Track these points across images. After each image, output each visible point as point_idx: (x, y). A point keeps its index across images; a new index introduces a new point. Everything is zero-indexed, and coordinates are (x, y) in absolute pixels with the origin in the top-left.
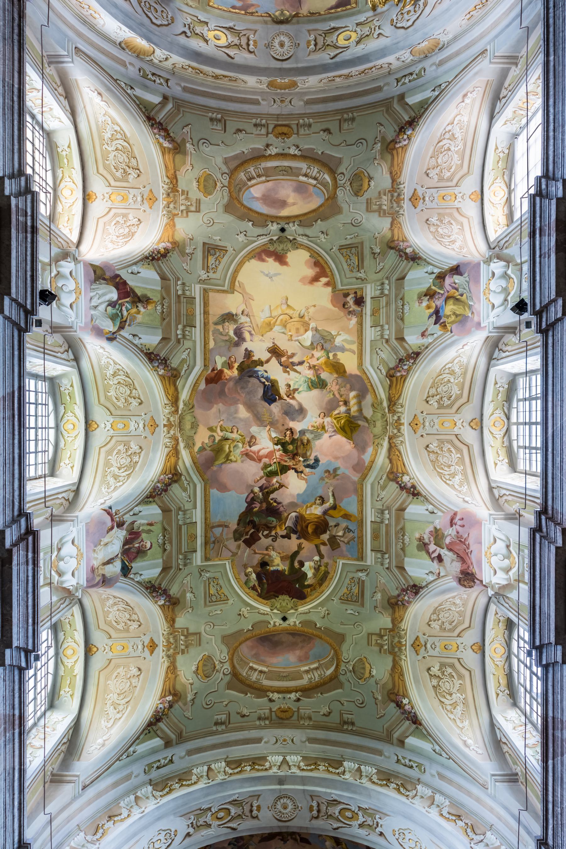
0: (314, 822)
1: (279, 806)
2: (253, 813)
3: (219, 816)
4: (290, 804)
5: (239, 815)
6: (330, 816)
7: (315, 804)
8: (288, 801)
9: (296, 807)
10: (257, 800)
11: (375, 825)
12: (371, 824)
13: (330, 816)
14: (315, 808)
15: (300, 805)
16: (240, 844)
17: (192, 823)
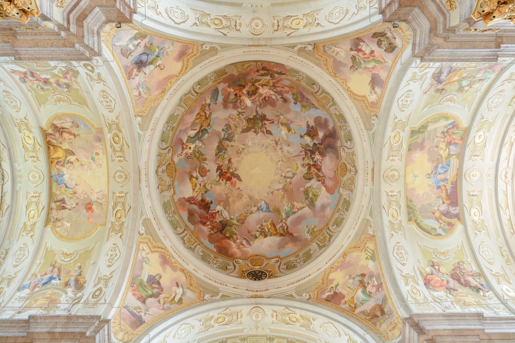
0: (275, 33)
1: (253, 25)
2: (237, 27)
3: (215, 23)
4: (260, 23)
5: (228, 26)
6: (285, 27)
7: (276, 22)
8: (259, 21)
9: (264, 25)
10: (240, 19)
11: (314, 21)
12: (311, 21)
13: (285, 27)
14: (276, 24)
15: (266, 24)
16: (229, 132)
17: (198, 18)
